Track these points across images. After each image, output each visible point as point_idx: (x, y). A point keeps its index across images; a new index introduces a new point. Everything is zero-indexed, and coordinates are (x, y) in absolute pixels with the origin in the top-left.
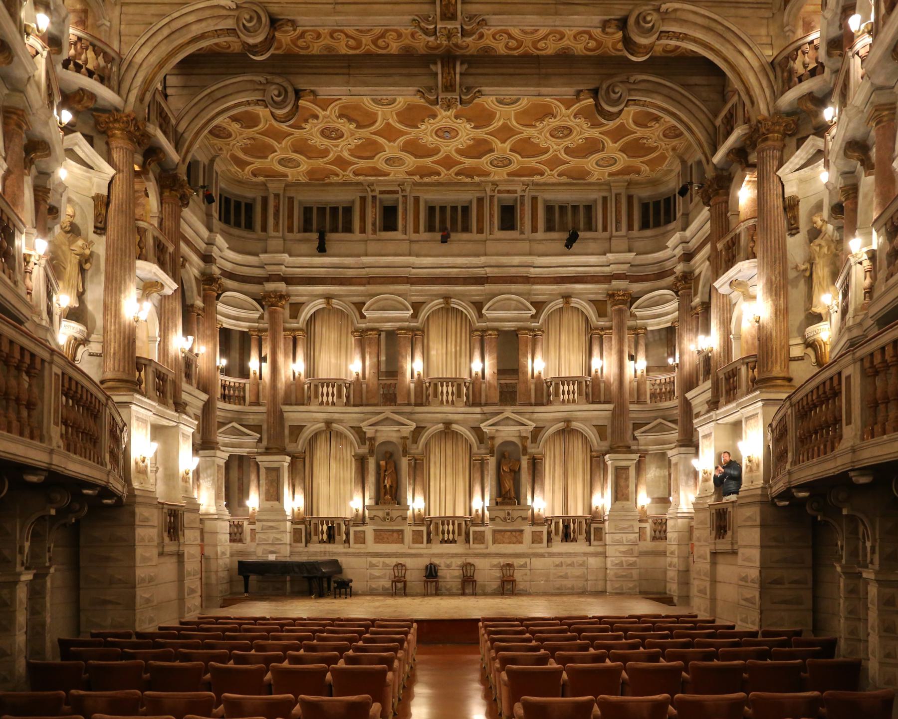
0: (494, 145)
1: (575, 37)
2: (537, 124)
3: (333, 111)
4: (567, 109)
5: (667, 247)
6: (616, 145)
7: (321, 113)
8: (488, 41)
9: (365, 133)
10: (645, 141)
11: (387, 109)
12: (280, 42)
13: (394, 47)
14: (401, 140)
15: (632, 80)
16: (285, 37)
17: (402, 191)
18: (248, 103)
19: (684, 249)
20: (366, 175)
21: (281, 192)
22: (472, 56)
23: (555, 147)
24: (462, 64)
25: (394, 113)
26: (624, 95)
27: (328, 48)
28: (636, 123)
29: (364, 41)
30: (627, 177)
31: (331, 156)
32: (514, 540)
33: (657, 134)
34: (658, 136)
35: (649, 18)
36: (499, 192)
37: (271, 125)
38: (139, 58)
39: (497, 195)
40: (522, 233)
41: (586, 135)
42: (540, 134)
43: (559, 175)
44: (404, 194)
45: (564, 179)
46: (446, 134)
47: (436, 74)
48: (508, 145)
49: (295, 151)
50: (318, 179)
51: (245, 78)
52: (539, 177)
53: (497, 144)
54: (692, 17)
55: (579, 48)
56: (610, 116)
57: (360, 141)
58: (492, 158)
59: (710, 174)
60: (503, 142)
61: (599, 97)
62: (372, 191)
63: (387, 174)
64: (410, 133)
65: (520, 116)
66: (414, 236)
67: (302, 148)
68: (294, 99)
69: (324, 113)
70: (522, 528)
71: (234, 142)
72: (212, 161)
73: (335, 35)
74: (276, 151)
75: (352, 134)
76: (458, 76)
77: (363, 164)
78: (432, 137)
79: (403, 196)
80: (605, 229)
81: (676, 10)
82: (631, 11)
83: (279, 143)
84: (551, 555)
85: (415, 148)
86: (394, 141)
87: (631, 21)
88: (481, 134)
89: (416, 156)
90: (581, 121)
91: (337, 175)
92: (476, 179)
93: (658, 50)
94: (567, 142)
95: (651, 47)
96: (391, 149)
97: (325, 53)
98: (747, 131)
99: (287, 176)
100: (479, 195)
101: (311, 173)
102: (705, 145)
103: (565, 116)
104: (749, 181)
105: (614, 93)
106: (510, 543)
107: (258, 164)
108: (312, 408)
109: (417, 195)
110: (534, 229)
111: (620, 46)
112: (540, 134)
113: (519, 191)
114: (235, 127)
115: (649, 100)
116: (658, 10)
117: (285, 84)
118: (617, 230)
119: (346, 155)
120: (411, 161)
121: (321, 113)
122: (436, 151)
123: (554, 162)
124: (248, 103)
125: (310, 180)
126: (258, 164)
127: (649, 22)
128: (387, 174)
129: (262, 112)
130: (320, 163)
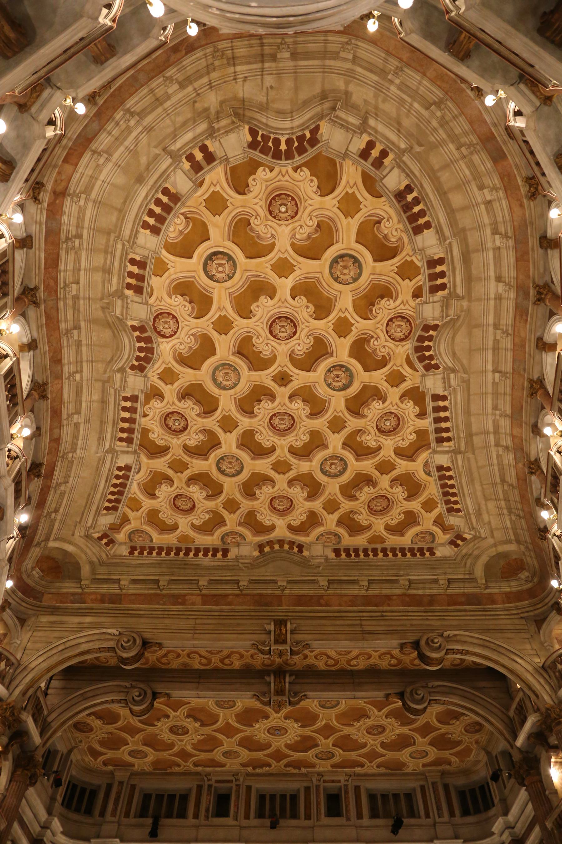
0: (318, 741)
1: (380, 657)
2: (355, 724)
3: (183, 711)
4: (380, 710)
5: (493, 834)
6: (425, 740)
7: (172, 713)
8: (311, 660)
9: (207, 730)
10: (450, 736)
11: (227, 711)
12: (147, 660)
13: (237, 664)
14: (238, 736)
15: (430, 685)
16: (151, 657)
17: (236, 780)
18: (113, 701)
19: (510, 834)
20: (205, 766)
21: (126, 780)
22: (298, 671)
23: (372, 742)
24: (290, 676)
25: (233, 715)
26: (426, 695)
27: (184, 664)
28: (439, 721)
29: (213, 661)
30: (440, 768)
31: (176, 749)
33: (459, 730)
34: (461, 731)
35: (436, 641)
36: (324, 781)
37: (128, 722)
38: (32, 665)
39: (322, 785)
40: (348, 819)
41: (398, 732)
42: (358, 731)
43: (378, 767)
44: (238, 783)
45: (382, 770)
46: (277, 732)
47: (270, 683)
48: (330, 741)
49: (145, 744)
50: (161, 769)
51: (115, 683)
52: (360, 768)
53: (321, 740)
54: (469, 639)
55: (384, 664)
56: (417, 712)
57: (203, 737)
58: (317, 751)
59: (517, 757)
60: (326, 738)
61: (406, 698)
62: (209, 780)
63: (224, 766)
64: (246, 731)
65: (339, 717)
66: (245, 823)
67: (152, 742)
68: (151, 699)
69: (174, 714)
71: (94, 736)
72: (70, 751)
73: (191, 656)
74: (128, 744)
75: (196, 731)
76: (287, 685)
77: (203, 756)
78: (264, 734)
79: (237, 785)
80: (427, 816)
81: (455, 635)
82: (421, 637)
83: (132, 737)
85: (249, 743)
86: (232, 737)
87: (423, 643)
88: (307, 731)
89: (250, 750)
90: (392, 720)
91: (179, 766)
92: (304, 770)
93: (447, 664)
94: (382, 738)
95: (440, 661)
96: (228, 744)
97: (182, 668)
98: (540, 718)
99: (133, 765)
100: (306, 784)
101: (156, 764)
102: (505, 732)
103: (377, 717)
104: (556, 762)
105: (417, 694)
107: (110, 754)
109: (250, 784)
110: (360, 816)
111: (417, 662)
112: (357, 731)
113: (342, 781)
114: (97, 723)
115: (447, 699)
116: (442, 635)
117: (146, 688)
118: (439, 817)
119: (189, 748)
120: (245, 754)
121: (172, 713)
122: (268, 746)
123: (372, 755)
124: (113, 701)
125: (154, 769)
126: (110, 754)
127: (437, 643)
128: (224, 766)
129: (124, 712)
130: (165, 755)
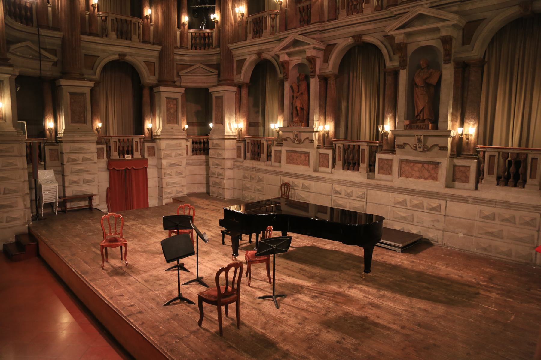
32: (427, 174)
70: (438, 160)
84: (477, 201)
106: (420, 177)
108: (247, 42)
